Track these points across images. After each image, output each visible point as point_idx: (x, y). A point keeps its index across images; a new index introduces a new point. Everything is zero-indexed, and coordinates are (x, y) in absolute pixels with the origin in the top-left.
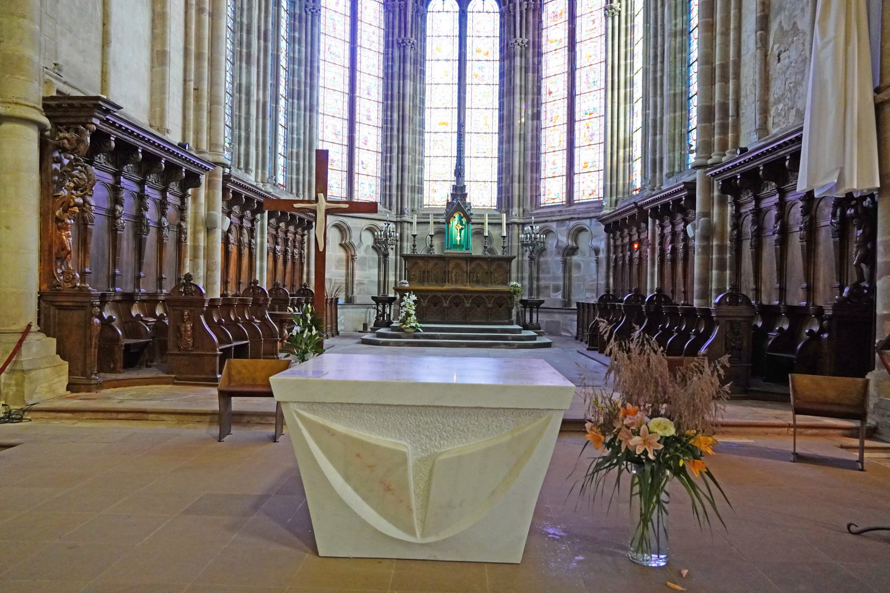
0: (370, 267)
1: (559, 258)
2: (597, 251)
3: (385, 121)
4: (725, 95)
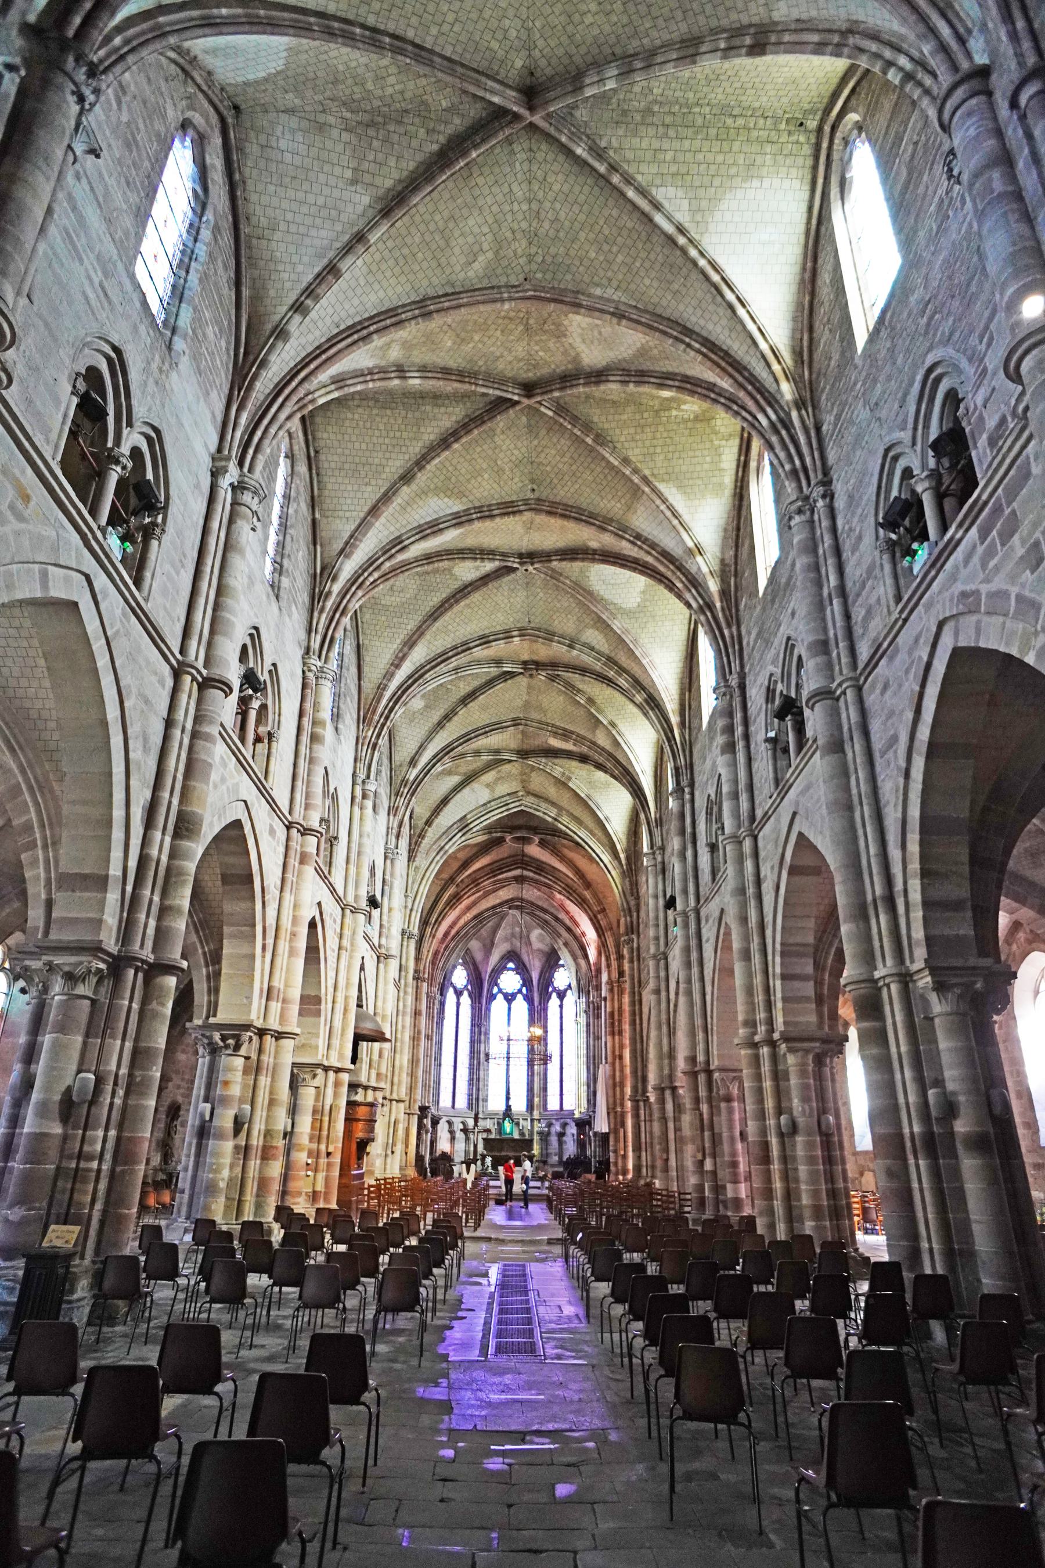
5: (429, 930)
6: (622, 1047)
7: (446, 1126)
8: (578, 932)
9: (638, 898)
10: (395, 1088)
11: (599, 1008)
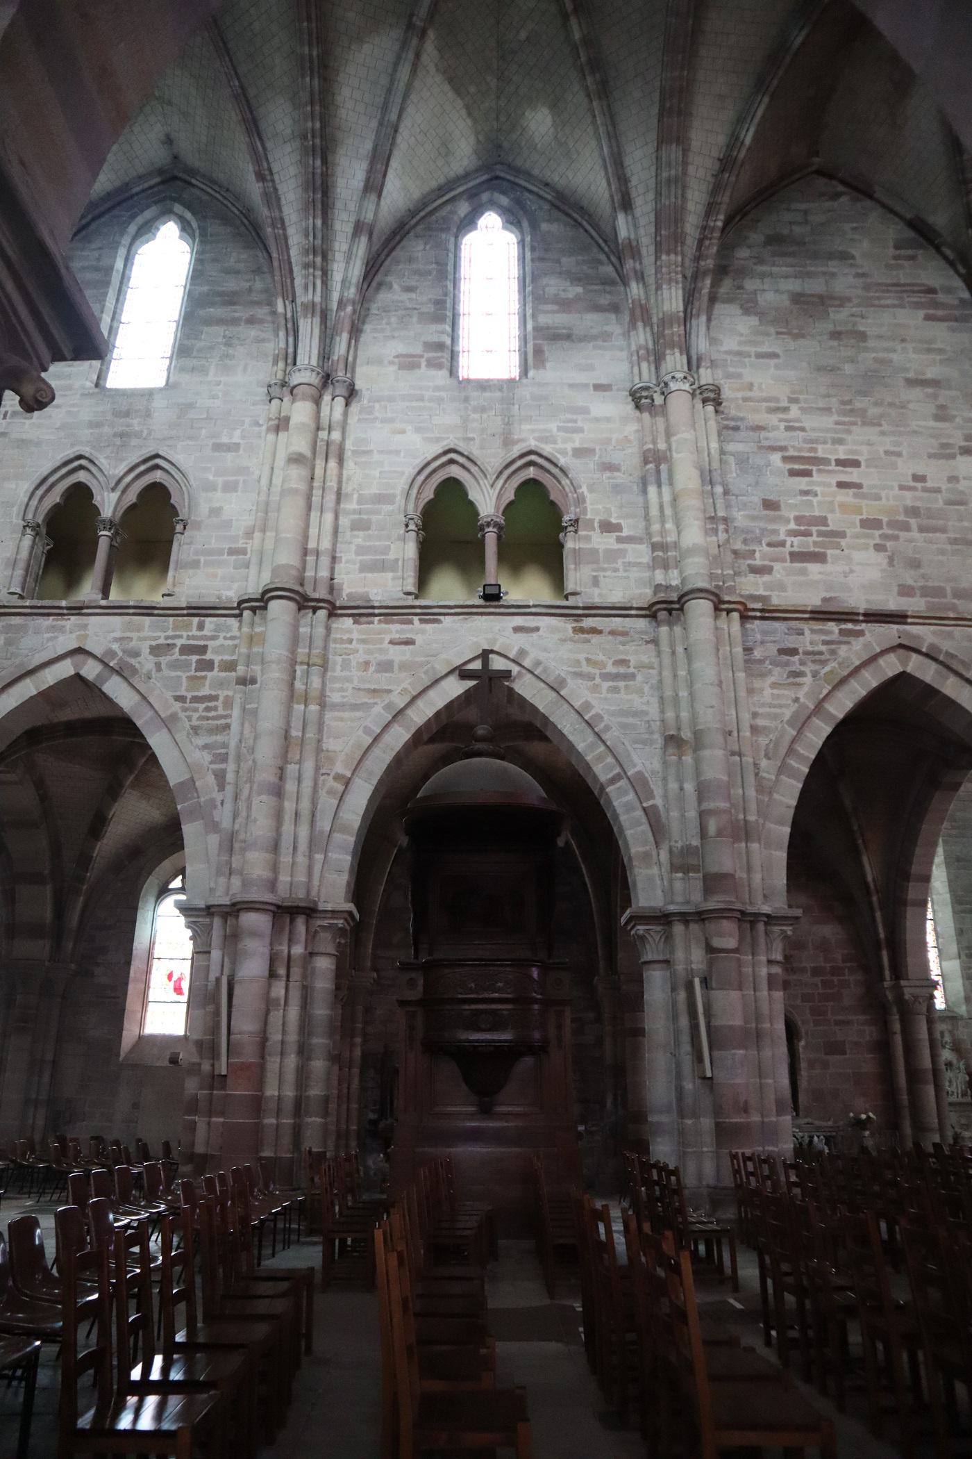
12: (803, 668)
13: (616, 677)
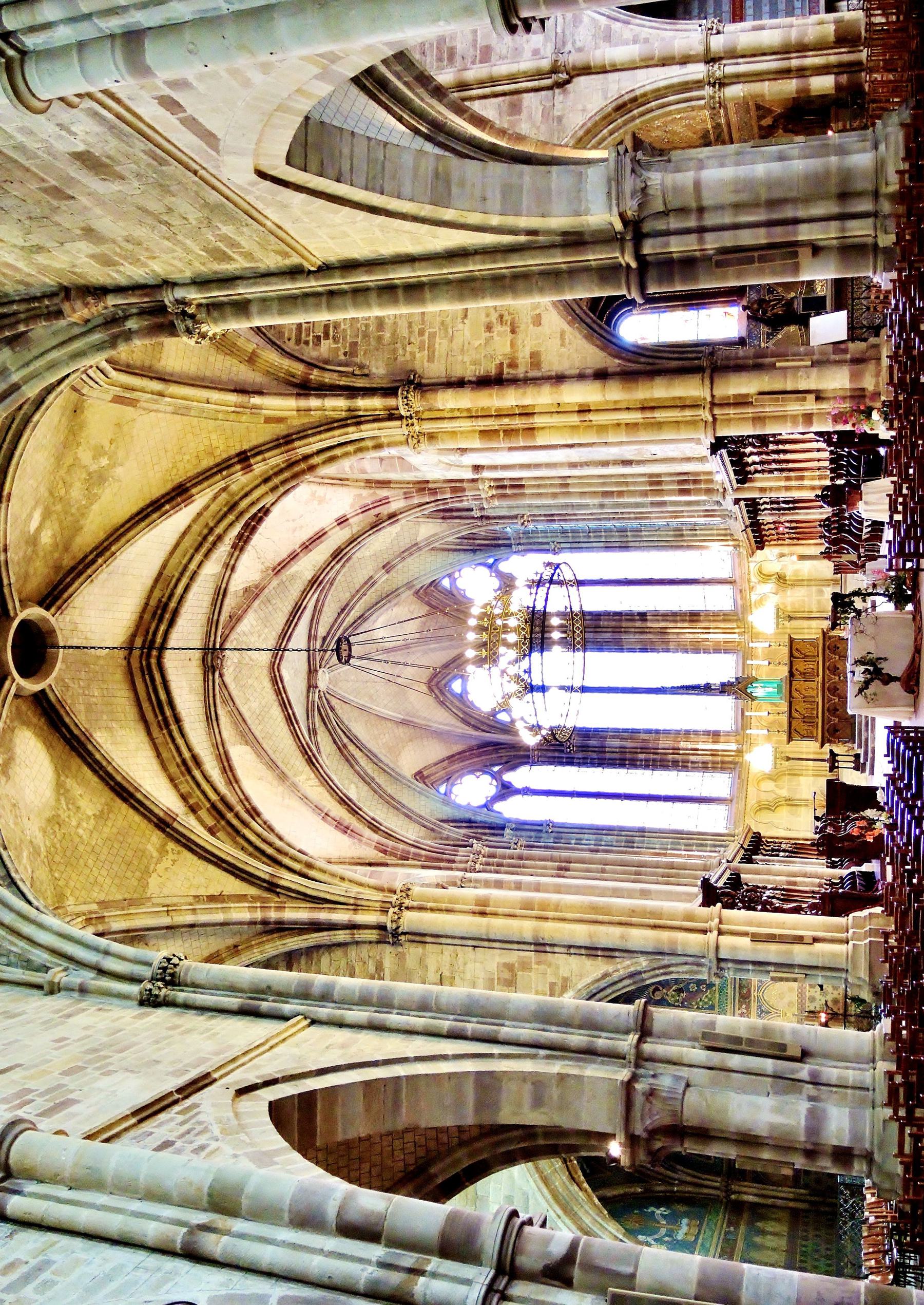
0: (799, 785)
1: (789, 592)
2: (782, 555)
3: (647, 767)
4: (672, 482)
5: (287, 879)
6: (560, 410)
7: (765, 816)
8: (338, 537)
9: (66, 292)
10: (602, 1042)
11: (500, 485)
12: (195, 1145)
13: (26, 1279)
